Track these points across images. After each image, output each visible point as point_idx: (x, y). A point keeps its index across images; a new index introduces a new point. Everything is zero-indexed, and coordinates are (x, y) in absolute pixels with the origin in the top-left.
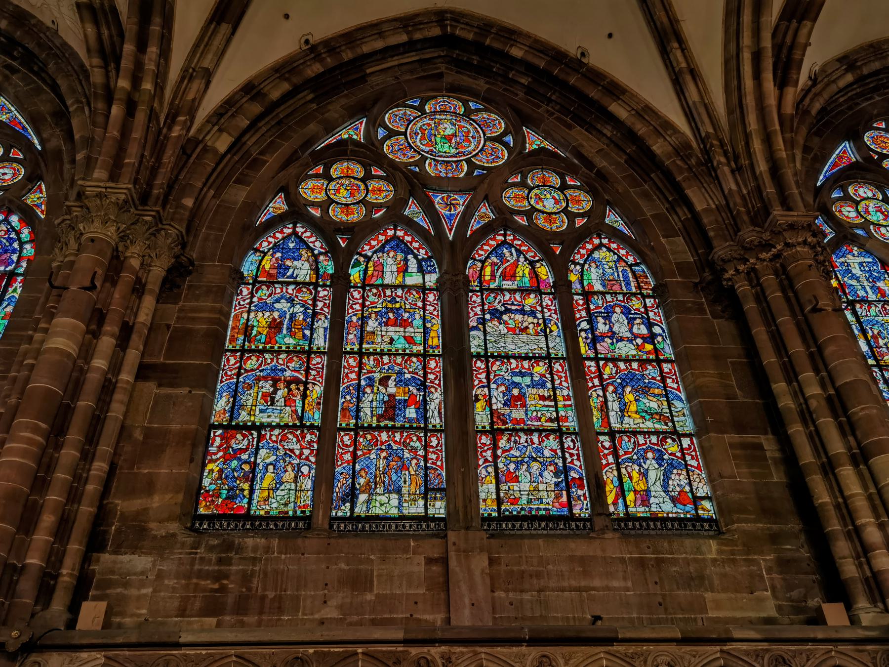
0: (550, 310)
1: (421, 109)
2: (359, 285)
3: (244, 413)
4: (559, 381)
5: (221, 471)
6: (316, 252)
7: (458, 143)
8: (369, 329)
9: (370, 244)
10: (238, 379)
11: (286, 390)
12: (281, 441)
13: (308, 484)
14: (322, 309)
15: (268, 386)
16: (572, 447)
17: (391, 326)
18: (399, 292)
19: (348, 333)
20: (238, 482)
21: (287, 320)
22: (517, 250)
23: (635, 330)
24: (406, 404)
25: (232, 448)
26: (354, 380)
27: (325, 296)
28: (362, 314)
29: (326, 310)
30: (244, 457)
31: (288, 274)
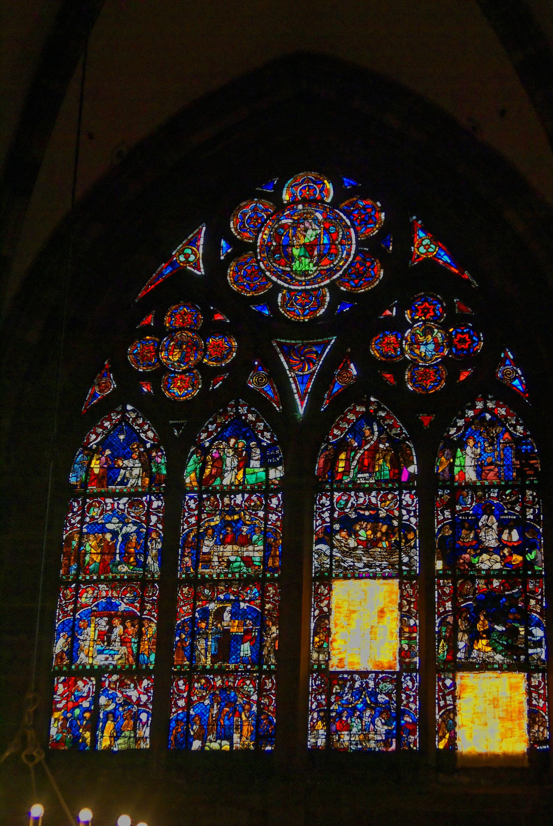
0: (409, 512)
1: (276, 198)
2: (196, 489)
3: (82, 655)
4: (408, 607)
5: (66, 719)
6: (148, 445)
7: (321, 256)
8: (205, 550)
9: (207, 430)
10: (74, 616)
11: (121, 627)
12: (119, 687)
13: (146, 732)
14: (155, 525)
15: (104, 624)
16: (410, 687)
17: (229, 544)
18: (239, 499)
19: (183, 556)
20: (81, 731)
21: (119, 543)
22: (379, 426)
23: (505, 537)
24: (241, 640)
25: (74, 695)
26: (189, 614)
27: (159, 507)
28: (198, 530)
29: (160, 526)
30: (86, 704)
31: (119, 480)
